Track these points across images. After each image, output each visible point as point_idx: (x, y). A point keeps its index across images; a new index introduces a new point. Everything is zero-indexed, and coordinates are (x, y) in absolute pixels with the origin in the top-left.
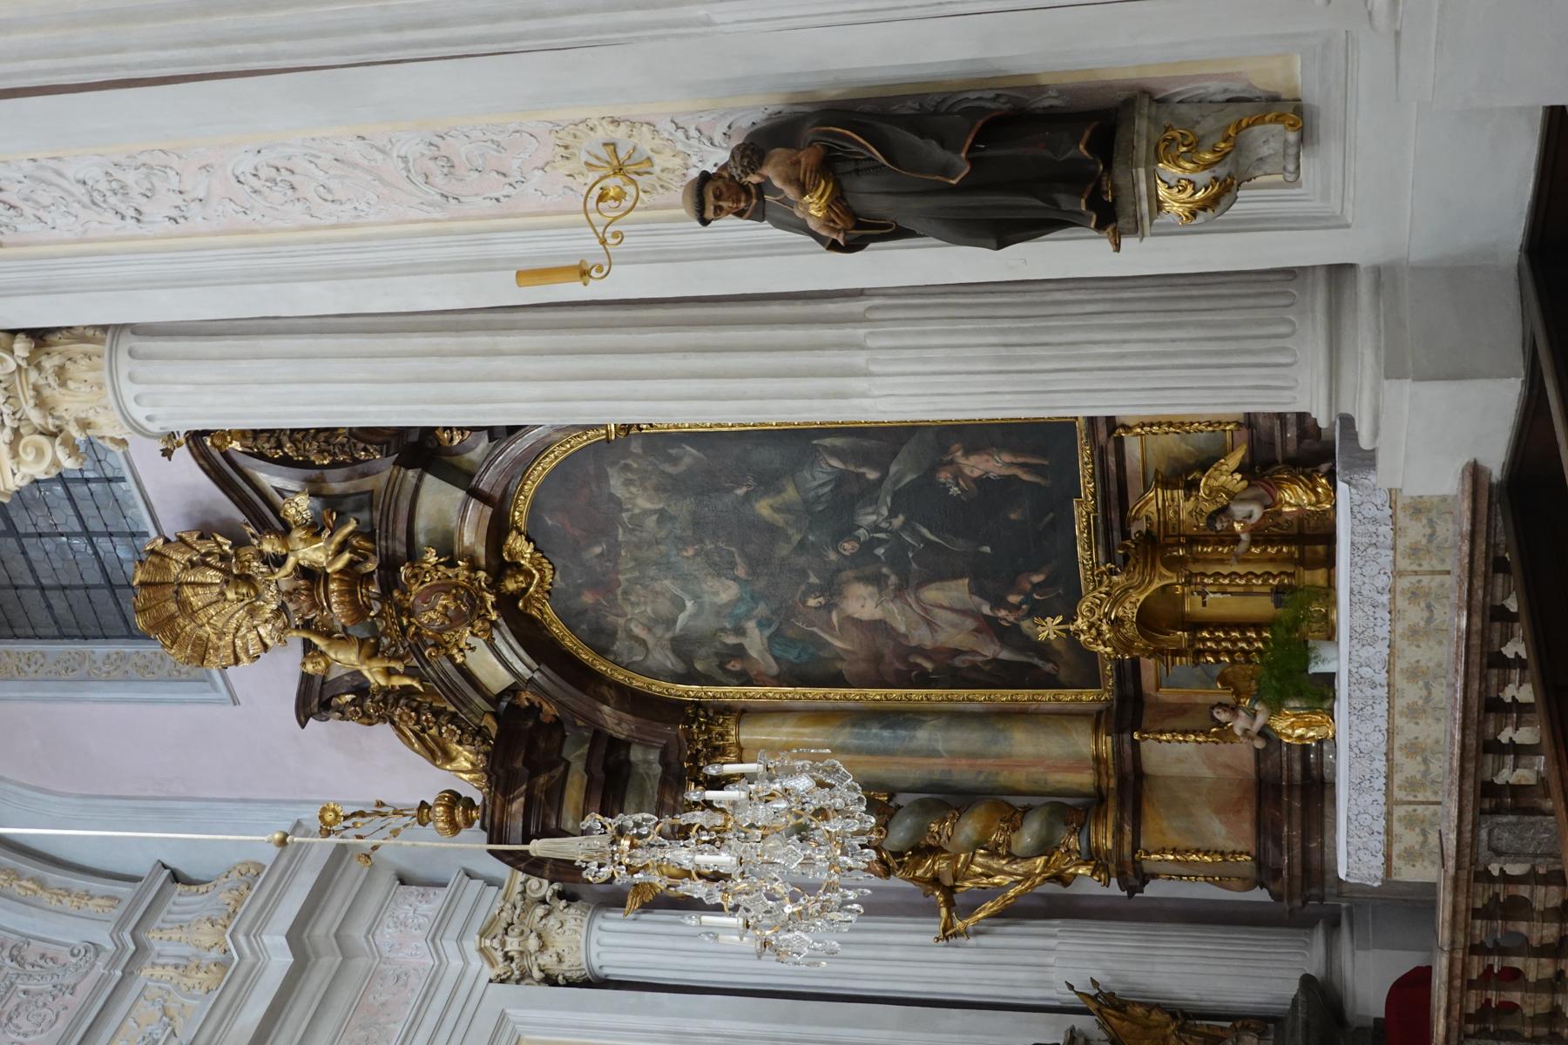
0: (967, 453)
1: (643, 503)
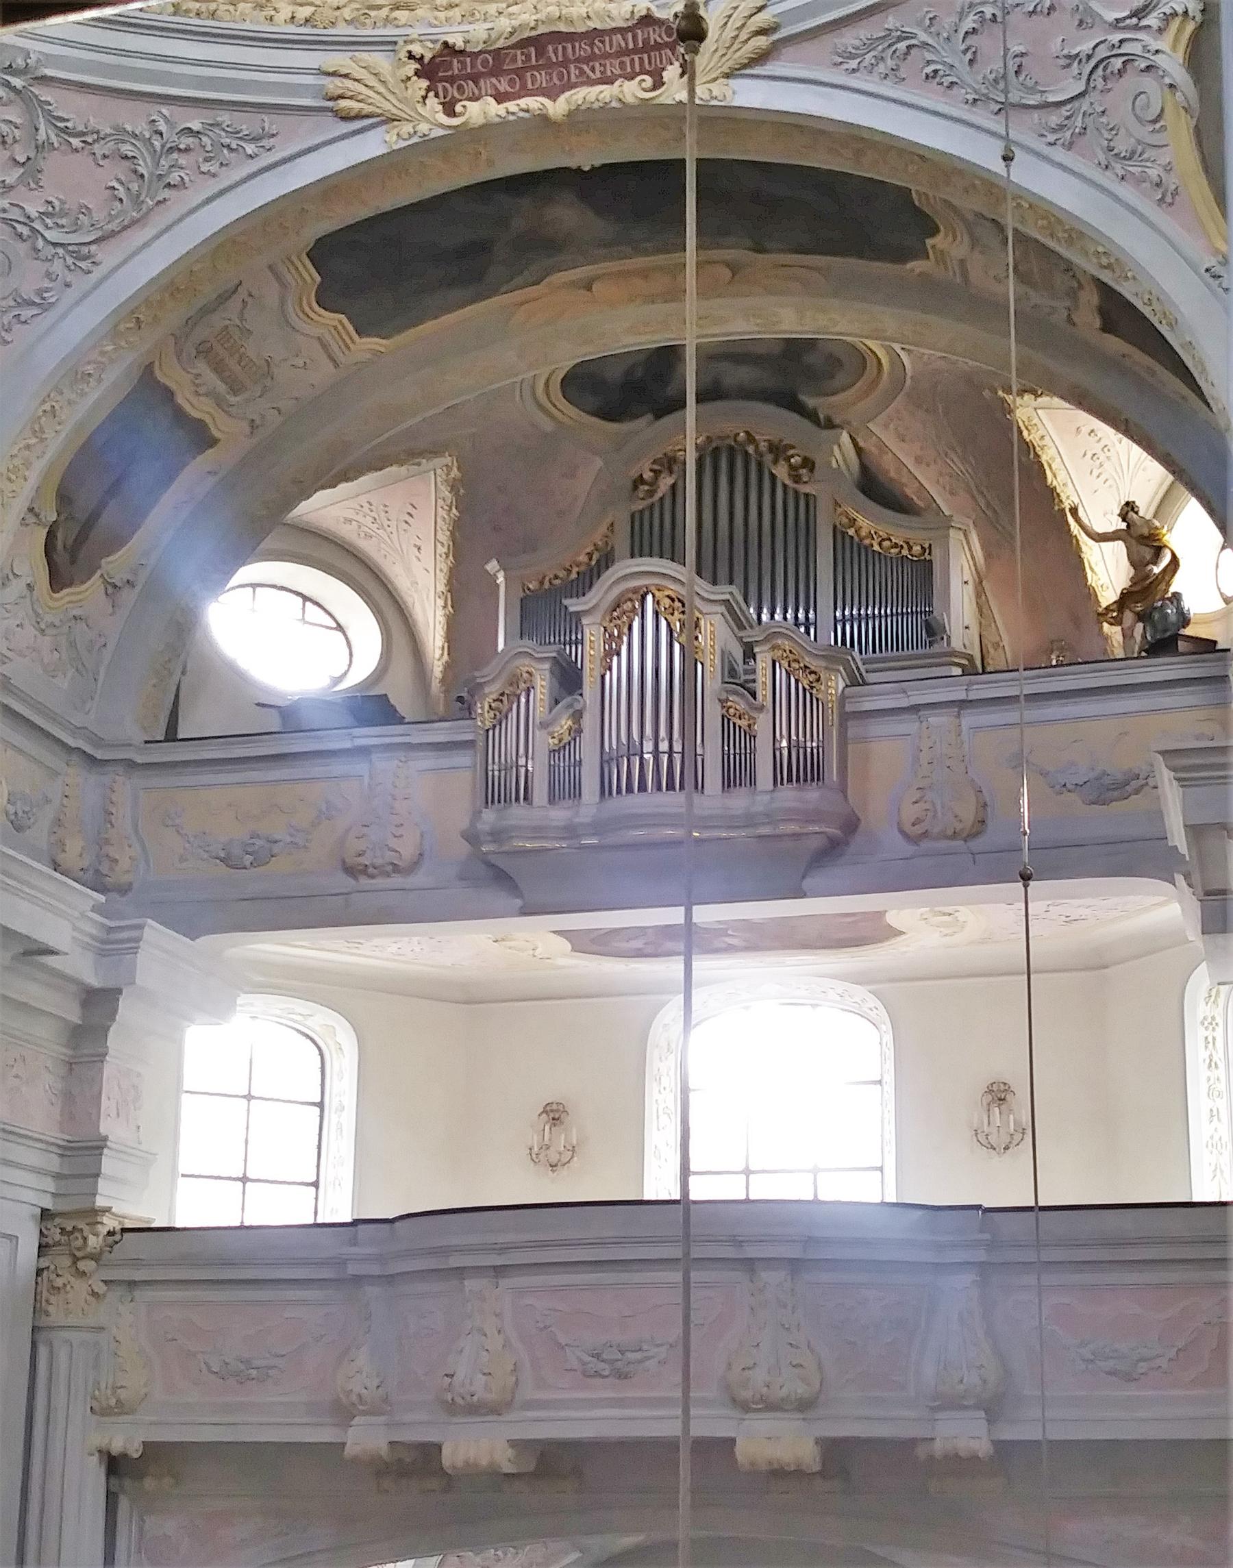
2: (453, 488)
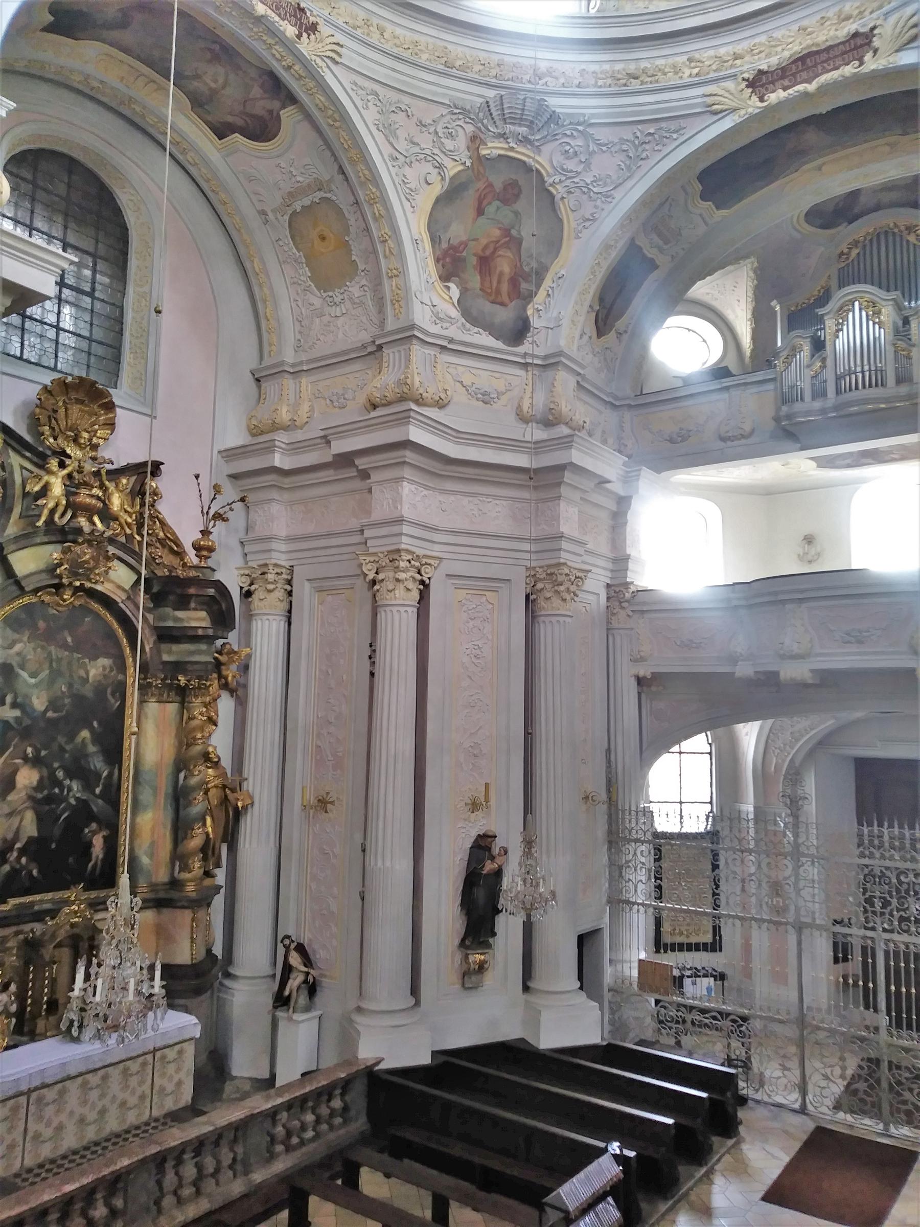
0: (104, 837)
1: (92, 672)
2: (755, 272)
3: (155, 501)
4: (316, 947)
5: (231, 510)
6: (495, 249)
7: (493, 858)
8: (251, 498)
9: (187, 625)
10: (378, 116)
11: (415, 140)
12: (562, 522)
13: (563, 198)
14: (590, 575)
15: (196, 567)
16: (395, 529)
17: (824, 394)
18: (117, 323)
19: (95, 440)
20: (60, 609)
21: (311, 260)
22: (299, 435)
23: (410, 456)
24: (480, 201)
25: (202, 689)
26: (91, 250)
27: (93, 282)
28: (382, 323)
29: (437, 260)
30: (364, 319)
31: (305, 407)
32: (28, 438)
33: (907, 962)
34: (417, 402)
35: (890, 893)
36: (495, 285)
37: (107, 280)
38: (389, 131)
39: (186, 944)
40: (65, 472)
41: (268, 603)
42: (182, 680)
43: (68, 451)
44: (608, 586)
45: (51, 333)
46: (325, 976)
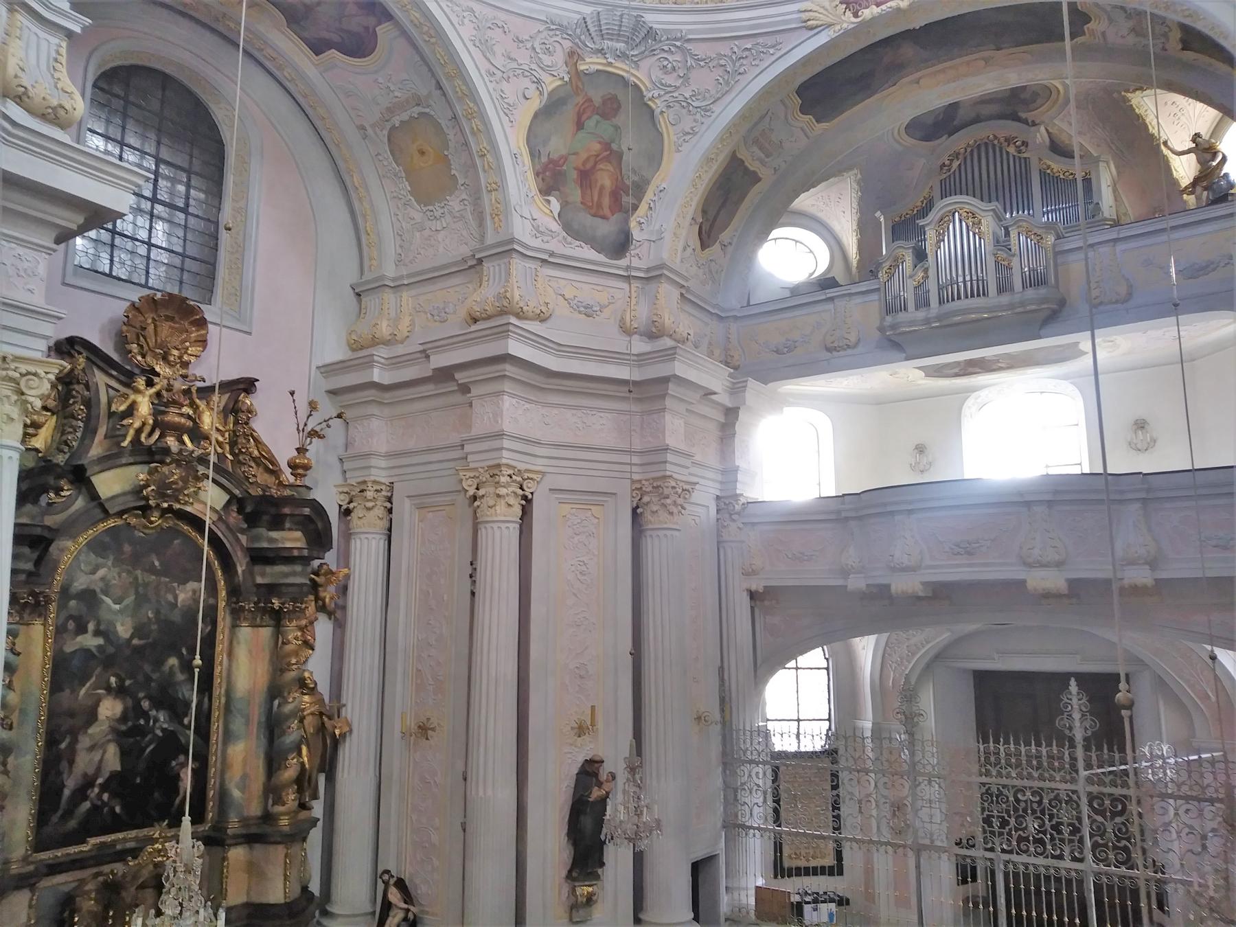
1: (182, 597)
3: (249, 418)
4: (417, 881)
5: (329, 426)
6: (596, 163)
7: (600, 784)
8: (348, 414)
9: (280, 545)
10: (474, 32)
11: (512, 55)
12: (667, 433)
13: (662, 112)
14: (697, 487)
15: (291, 486)
16: (495, 444)
17: (927, 304)
18: (212, 240)
19: (186, 358)
20: (147, 531)
21: (410, 174)
22: (400, 350)
23: (509, 369)
24: (579, 115)
25: (298, 613)
26: (186, 165)
27: (187, 197)
28: (483, 237)
29: (537, 174)
30: (464, 233)
31: (405, 322)
32: (115, 356)
33: (1027, 884)
34: (518, 316)
35: (1008, 812)
36: (596, 199)
37: (202, 196)
38: (485, 47)
39: (279, 884)
40: (152, 391)
41: (368, 523)
42: (276, 603)
43: (158, 369)
44: (718, 498)
45: (142, 250)
46: (427, 913)
